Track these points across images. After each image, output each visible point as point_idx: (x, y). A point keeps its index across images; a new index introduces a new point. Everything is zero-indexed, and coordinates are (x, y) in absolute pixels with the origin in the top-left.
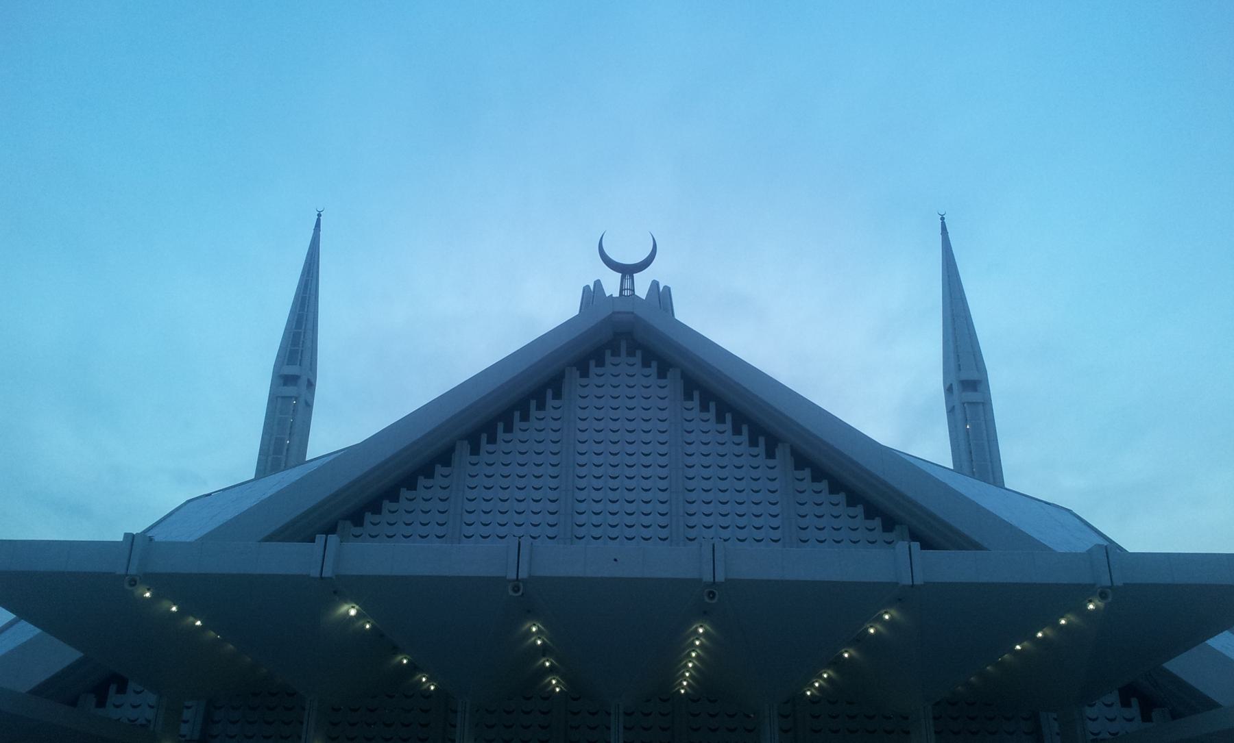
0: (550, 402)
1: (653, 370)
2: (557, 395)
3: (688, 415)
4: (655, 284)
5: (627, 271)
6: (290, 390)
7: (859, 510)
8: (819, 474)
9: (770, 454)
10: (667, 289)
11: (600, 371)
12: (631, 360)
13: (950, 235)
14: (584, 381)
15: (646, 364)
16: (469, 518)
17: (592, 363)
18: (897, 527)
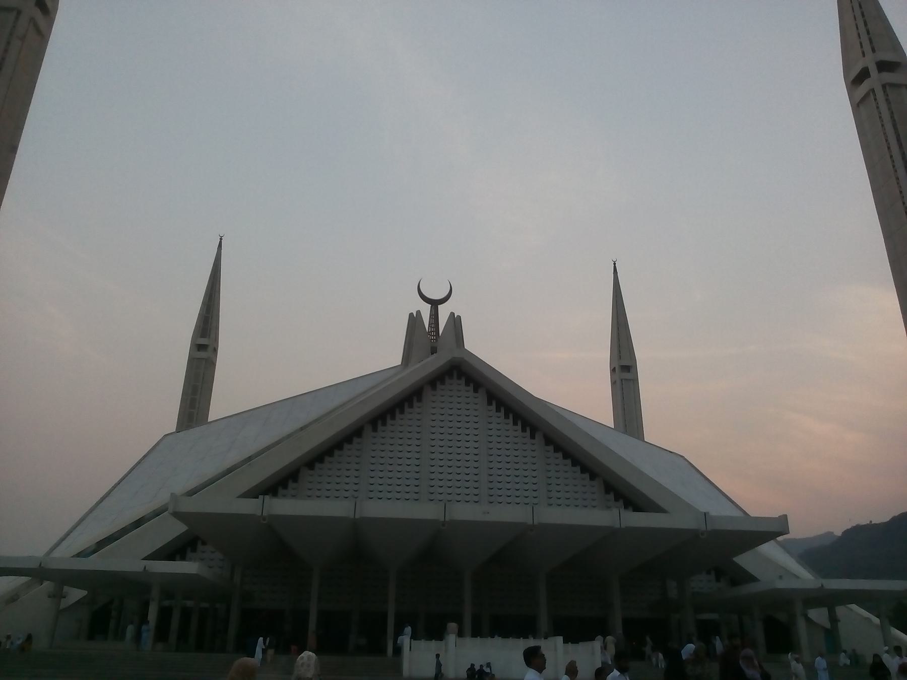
0: (416, 404)
1: (471, 388)
2: (420, 400)
4: (452, 314)
5: (435, 304)
6: (202, 354)
7: (578, 469)
8: (558, 449)
10: (459, 317)
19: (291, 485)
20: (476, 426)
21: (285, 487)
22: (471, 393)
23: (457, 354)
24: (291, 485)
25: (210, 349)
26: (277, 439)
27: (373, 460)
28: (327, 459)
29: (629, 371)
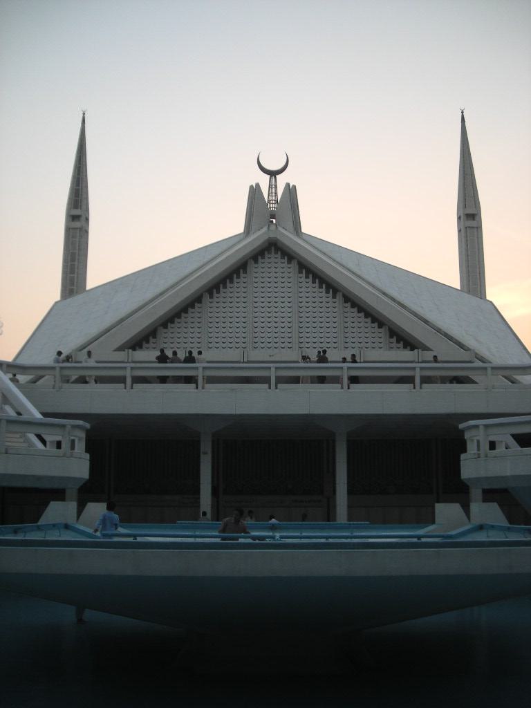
0: (242, 275)
2: (245, 272)
3: (300, 280)
4: (288, 185)
5: (273, 174)
6: (77, 224)
8: (354, 305)
10: (294, 187)
11: (263, 261)
14: (256, 266)
15: (283, 258)
16: (211, 325)
17: (260, 257)
19: (152, 340)
20: (289, 290)
21: (148, 342)
22: (285, 265)
23: (272, 235)
24: (152, 340)
25: (83, 218)
27: (210, 320)
28: (177, 320)
29: (474, 219)
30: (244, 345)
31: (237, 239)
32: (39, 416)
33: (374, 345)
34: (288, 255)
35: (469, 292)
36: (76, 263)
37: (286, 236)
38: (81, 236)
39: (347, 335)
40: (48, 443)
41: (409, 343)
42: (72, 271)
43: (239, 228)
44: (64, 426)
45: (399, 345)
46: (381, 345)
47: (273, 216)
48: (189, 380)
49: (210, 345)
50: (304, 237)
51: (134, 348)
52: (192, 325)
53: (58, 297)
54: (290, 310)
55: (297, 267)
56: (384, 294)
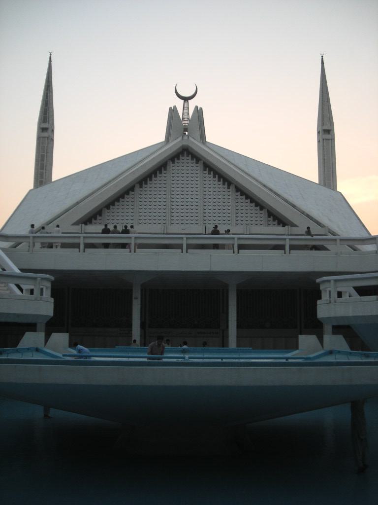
0: (163, 171)
2: (165, 169)
3: (205, 175)
4: (197, 107)
5: (186, 99)
6: (45, 134)
7: (253, 204)
8: (243, 193)
9: (229, 188)
10: (201, 109)
12: (188, 158)
13: (325, 64)
14: (173, 165)
16: (140, 207)
17: (176, 159)
18: (264, 209)
19: (99, 218)
21: (96, 219)
22: (194, 164)
23: (185, 143)
24: (99, 218)
25: (50, 130)
26: (91, 191)
28: (116, 203)
29: (329, 134)
30: (164, 222)
31: (159, 146)
32: (17, 271)
33: (257, 223)
34: (196, 158)
35: (325, 185)
36: (45, 162)
37: (195, 144)
38: (48, 143)
39: (237, 215)
40: (24, 291)
41: (281, 221)
42: (42, 168)
43: (161, 138)
44: (35, 279)
45: (274, 223)
46: (261, 223)
47: (186, 130)
48: (124, 246)
49: (140, 222)
50: (207, 144)
51: (86, 224)
52: (128, 207)
53: (32, 187)
54: (197, 197)
55: (202, 166)
56: (264, 186)
